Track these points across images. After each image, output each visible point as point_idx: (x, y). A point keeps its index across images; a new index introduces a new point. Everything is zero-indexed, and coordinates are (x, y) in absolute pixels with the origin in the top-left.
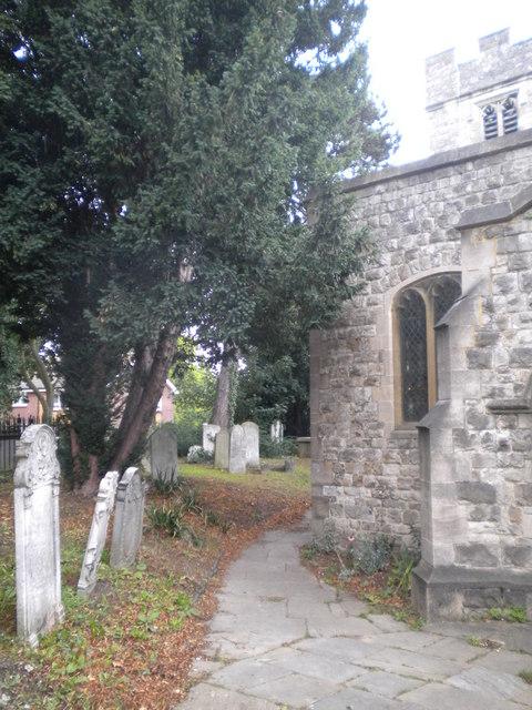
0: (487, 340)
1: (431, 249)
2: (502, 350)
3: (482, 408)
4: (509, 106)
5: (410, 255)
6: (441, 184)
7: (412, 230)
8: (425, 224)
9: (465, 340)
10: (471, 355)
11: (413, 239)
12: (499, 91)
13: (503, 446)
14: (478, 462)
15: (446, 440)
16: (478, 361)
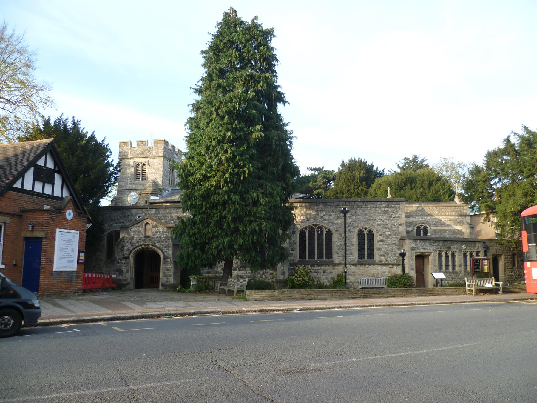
0: (123, 247)
1: (116, 225)
2: (126, 248)
3: (122, 257)
4: (144, 165)
5: (111, 225)
6: (119, 212)
7: (112, 220)
8: (115, 220)
9: (120, 247)
10: (120, 249)
11: (112, 222)
12: (142, 159)
13: (124, 263)
14: (120, 266)
15: (116, 262)
16: (122, 250)
